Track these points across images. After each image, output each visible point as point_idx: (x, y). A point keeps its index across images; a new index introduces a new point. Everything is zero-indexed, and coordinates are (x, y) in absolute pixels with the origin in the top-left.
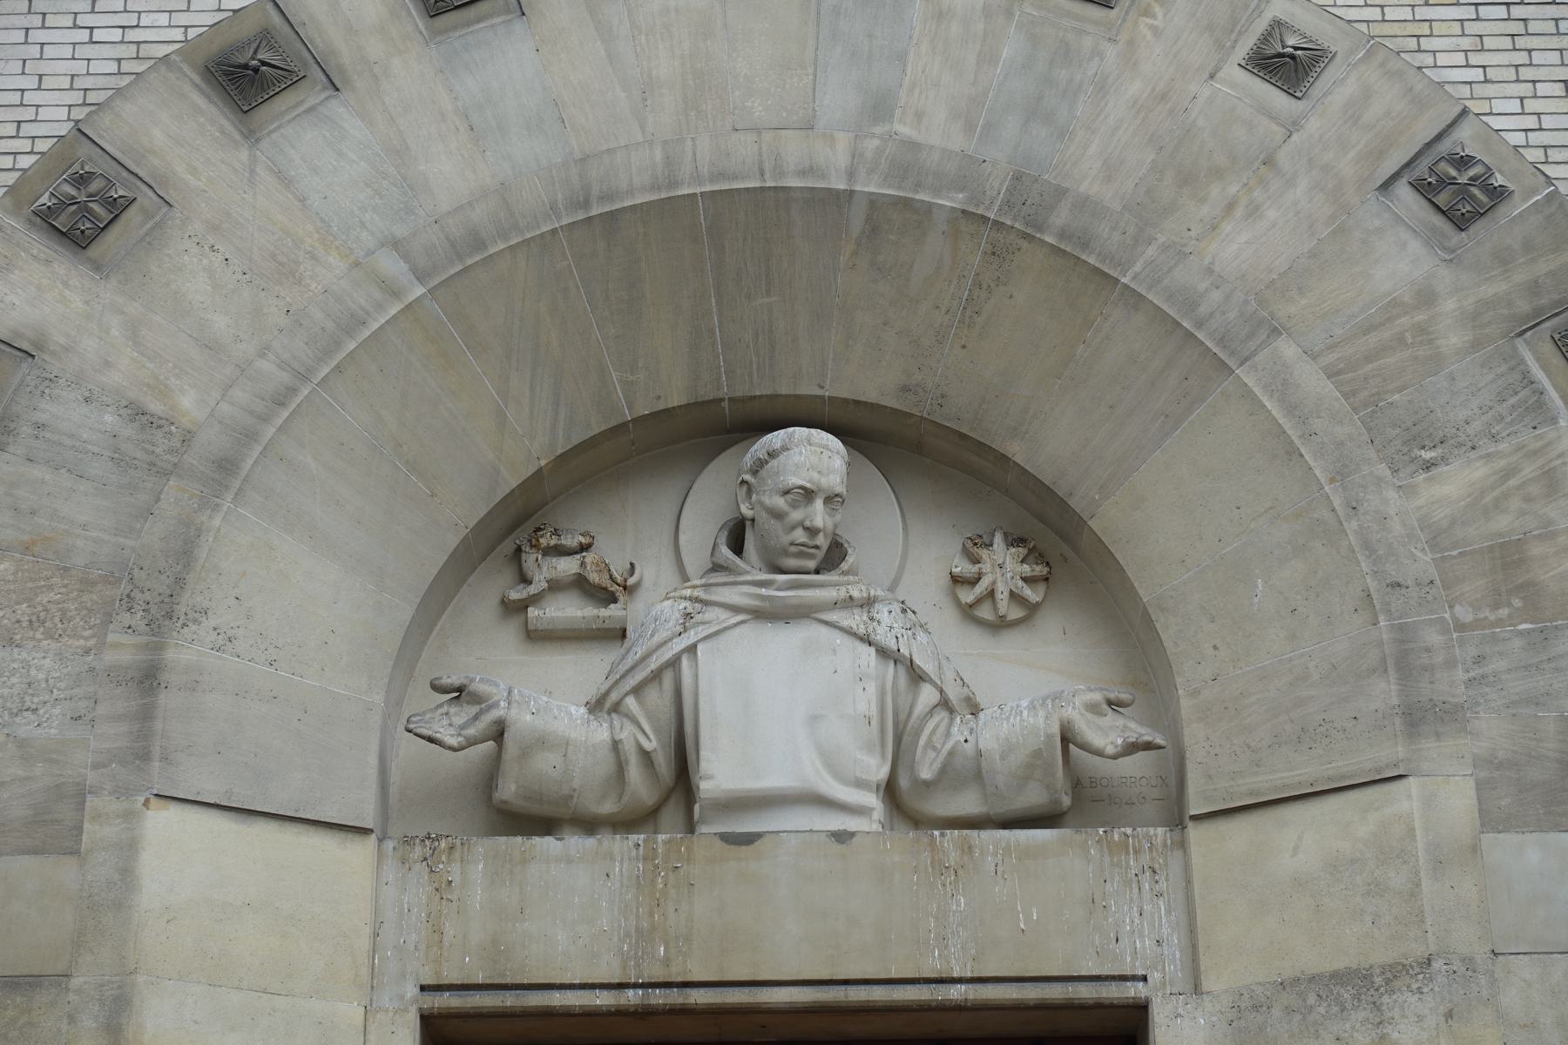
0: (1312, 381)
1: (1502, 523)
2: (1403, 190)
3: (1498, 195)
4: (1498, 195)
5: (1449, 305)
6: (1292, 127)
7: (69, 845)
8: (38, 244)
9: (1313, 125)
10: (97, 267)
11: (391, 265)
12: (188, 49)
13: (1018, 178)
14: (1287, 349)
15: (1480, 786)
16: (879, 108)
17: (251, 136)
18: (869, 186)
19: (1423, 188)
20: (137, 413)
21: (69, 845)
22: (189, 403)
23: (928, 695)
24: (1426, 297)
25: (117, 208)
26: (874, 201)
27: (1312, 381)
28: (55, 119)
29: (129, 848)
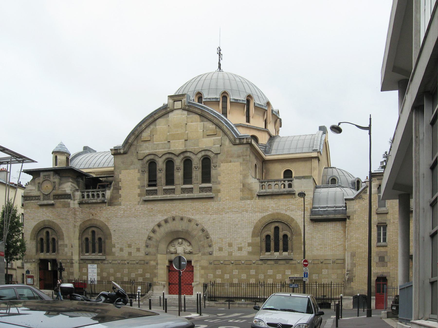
0: (197, 239)
1: (203, 244)
2: (201, 230)
3: (205, 231)
4: (205, 231)
5: (202, 235)
6: (197, 227)
7: (155, 255)
8: (152, 233)
9: (198, 228)
10: (154, 234)
11: (164, 234)
12: (157, 224)
13: (187, 230)
14: (196, 237)
15: (201, 254)
16: (182, 227)
17: (159, 228)
18: (181, 230)
19: (202, 230)
20: (156, 240)
21: (155, 255)
22: (158, 239)
23: (185, 249)
24: (201, 235)
25: (155, 231)
26: (182, 231)
27: (197, 239)
28: (152, 228)
29: (157, 256)
